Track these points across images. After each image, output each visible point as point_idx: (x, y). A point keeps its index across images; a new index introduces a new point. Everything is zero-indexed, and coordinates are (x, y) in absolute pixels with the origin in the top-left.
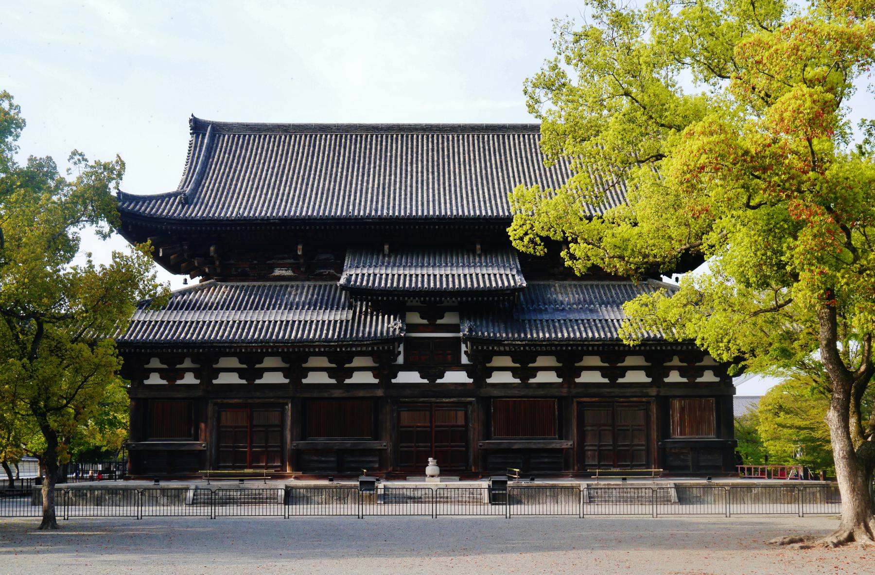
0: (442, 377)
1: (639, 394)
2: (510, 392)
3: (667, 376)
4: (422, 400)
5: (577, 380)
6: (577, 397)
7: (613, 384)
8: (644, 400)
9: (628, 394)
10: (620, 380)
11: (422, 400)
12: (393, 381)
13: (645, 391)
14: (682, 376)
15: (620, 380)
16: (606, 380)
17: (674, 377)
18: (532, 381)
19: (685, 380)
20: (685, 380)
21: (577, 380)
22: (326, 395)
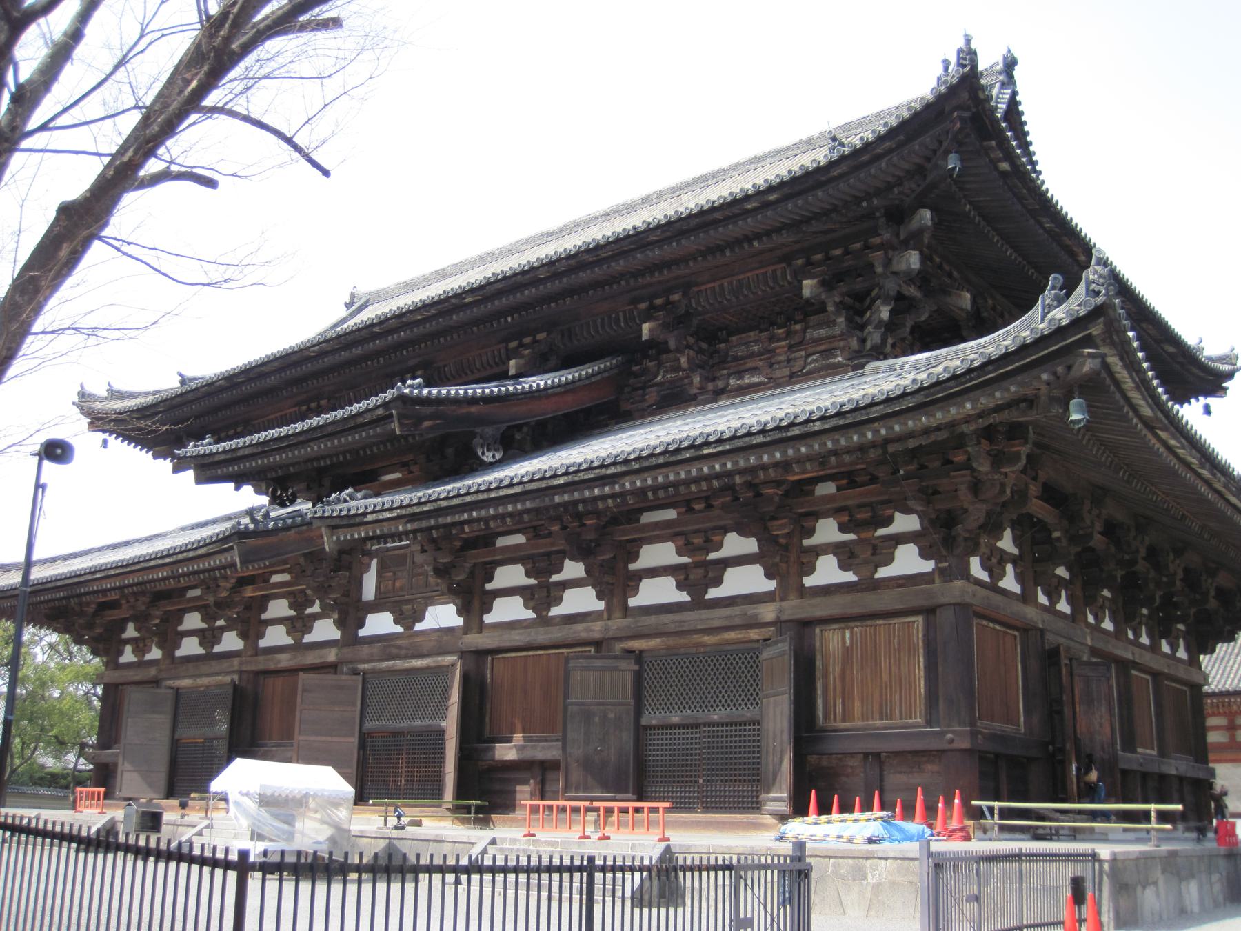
0: (421, 618)
1: (738, 621)
2: (518, 638)
3: (811, 570)
4: (385, 664)
5: (633, 602)
6: (620, 639)
7: (699, 603)
8: (754, 634)
9: (716, 624)
10: (713, 593)
11: (385, 664)
12: (362, 633)
13: (751, 610)
14: (843, 566)
15: (713, 593)
16: (684, 597)
17: (827, 572)
18: (555, 611)
19: (849, 577)
20: (849, 577)
21: (633, 602)
22: (272, 666)
